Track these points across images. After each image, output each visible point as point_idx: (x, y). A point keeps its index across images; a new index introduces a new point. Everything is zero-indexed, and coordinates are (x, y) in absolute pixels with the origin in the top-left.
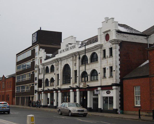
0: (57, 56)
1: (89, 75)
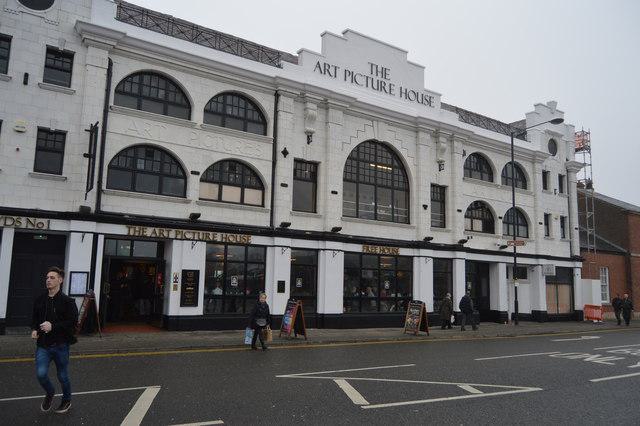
0: (287, 72)
1: (500, 218)
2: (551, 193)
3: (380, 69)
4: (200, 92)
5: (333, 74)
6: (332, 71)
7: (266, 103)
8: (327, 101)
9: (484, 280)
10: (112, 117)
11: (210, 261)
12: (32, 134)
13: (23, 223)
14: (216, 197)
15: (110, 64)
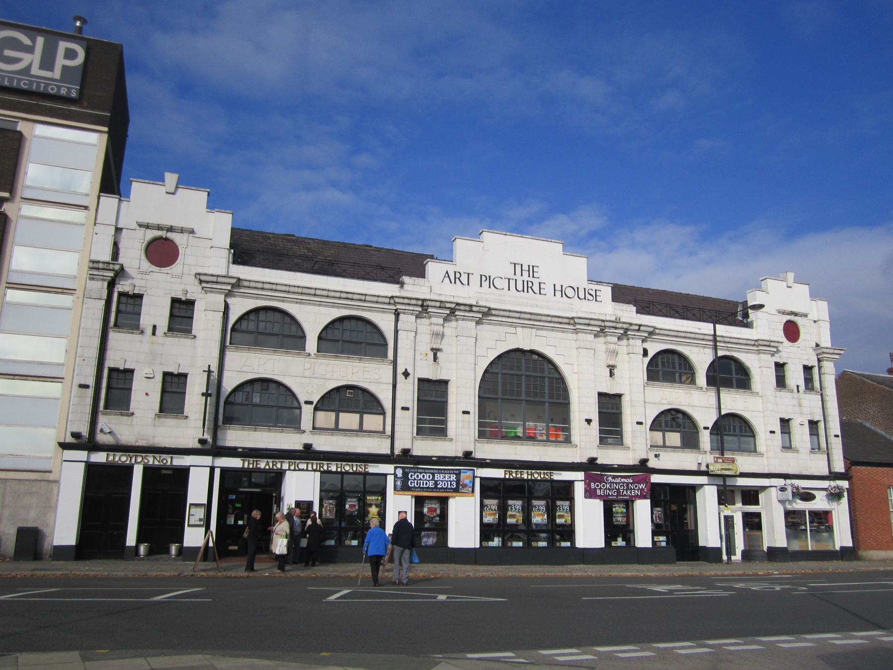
0: (413, 287)
1: (706, 428)
2: (792, 391)
3: (525, 268)
4: (313, 320)
5: (465, 282)
6: (464, 279)
7: (384, 322)
8: (453, 311)
9: (690, 507)
10: (230, 355)
11: (325, 492)
12: (159, 378)
13: (151, 460)
14: (333, 426)
15: (227, 307)
